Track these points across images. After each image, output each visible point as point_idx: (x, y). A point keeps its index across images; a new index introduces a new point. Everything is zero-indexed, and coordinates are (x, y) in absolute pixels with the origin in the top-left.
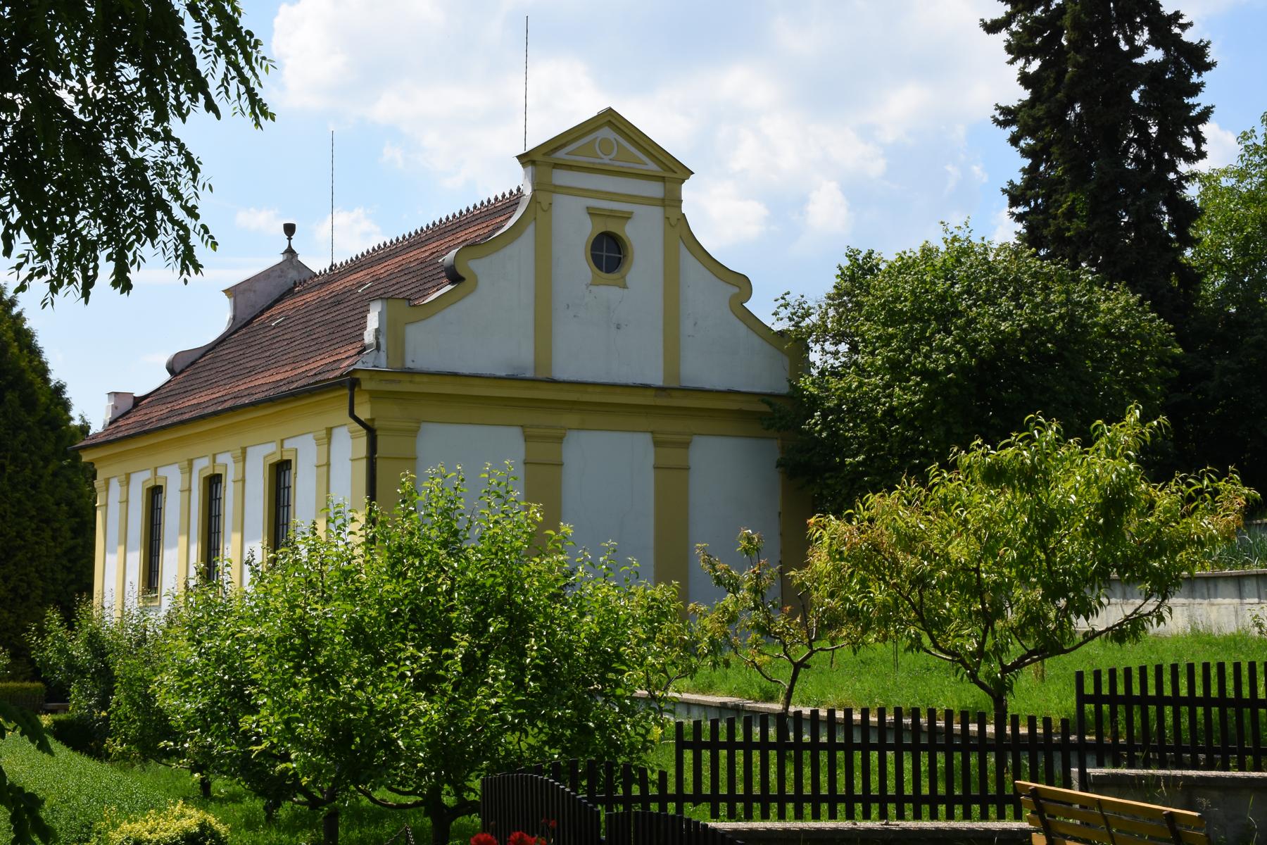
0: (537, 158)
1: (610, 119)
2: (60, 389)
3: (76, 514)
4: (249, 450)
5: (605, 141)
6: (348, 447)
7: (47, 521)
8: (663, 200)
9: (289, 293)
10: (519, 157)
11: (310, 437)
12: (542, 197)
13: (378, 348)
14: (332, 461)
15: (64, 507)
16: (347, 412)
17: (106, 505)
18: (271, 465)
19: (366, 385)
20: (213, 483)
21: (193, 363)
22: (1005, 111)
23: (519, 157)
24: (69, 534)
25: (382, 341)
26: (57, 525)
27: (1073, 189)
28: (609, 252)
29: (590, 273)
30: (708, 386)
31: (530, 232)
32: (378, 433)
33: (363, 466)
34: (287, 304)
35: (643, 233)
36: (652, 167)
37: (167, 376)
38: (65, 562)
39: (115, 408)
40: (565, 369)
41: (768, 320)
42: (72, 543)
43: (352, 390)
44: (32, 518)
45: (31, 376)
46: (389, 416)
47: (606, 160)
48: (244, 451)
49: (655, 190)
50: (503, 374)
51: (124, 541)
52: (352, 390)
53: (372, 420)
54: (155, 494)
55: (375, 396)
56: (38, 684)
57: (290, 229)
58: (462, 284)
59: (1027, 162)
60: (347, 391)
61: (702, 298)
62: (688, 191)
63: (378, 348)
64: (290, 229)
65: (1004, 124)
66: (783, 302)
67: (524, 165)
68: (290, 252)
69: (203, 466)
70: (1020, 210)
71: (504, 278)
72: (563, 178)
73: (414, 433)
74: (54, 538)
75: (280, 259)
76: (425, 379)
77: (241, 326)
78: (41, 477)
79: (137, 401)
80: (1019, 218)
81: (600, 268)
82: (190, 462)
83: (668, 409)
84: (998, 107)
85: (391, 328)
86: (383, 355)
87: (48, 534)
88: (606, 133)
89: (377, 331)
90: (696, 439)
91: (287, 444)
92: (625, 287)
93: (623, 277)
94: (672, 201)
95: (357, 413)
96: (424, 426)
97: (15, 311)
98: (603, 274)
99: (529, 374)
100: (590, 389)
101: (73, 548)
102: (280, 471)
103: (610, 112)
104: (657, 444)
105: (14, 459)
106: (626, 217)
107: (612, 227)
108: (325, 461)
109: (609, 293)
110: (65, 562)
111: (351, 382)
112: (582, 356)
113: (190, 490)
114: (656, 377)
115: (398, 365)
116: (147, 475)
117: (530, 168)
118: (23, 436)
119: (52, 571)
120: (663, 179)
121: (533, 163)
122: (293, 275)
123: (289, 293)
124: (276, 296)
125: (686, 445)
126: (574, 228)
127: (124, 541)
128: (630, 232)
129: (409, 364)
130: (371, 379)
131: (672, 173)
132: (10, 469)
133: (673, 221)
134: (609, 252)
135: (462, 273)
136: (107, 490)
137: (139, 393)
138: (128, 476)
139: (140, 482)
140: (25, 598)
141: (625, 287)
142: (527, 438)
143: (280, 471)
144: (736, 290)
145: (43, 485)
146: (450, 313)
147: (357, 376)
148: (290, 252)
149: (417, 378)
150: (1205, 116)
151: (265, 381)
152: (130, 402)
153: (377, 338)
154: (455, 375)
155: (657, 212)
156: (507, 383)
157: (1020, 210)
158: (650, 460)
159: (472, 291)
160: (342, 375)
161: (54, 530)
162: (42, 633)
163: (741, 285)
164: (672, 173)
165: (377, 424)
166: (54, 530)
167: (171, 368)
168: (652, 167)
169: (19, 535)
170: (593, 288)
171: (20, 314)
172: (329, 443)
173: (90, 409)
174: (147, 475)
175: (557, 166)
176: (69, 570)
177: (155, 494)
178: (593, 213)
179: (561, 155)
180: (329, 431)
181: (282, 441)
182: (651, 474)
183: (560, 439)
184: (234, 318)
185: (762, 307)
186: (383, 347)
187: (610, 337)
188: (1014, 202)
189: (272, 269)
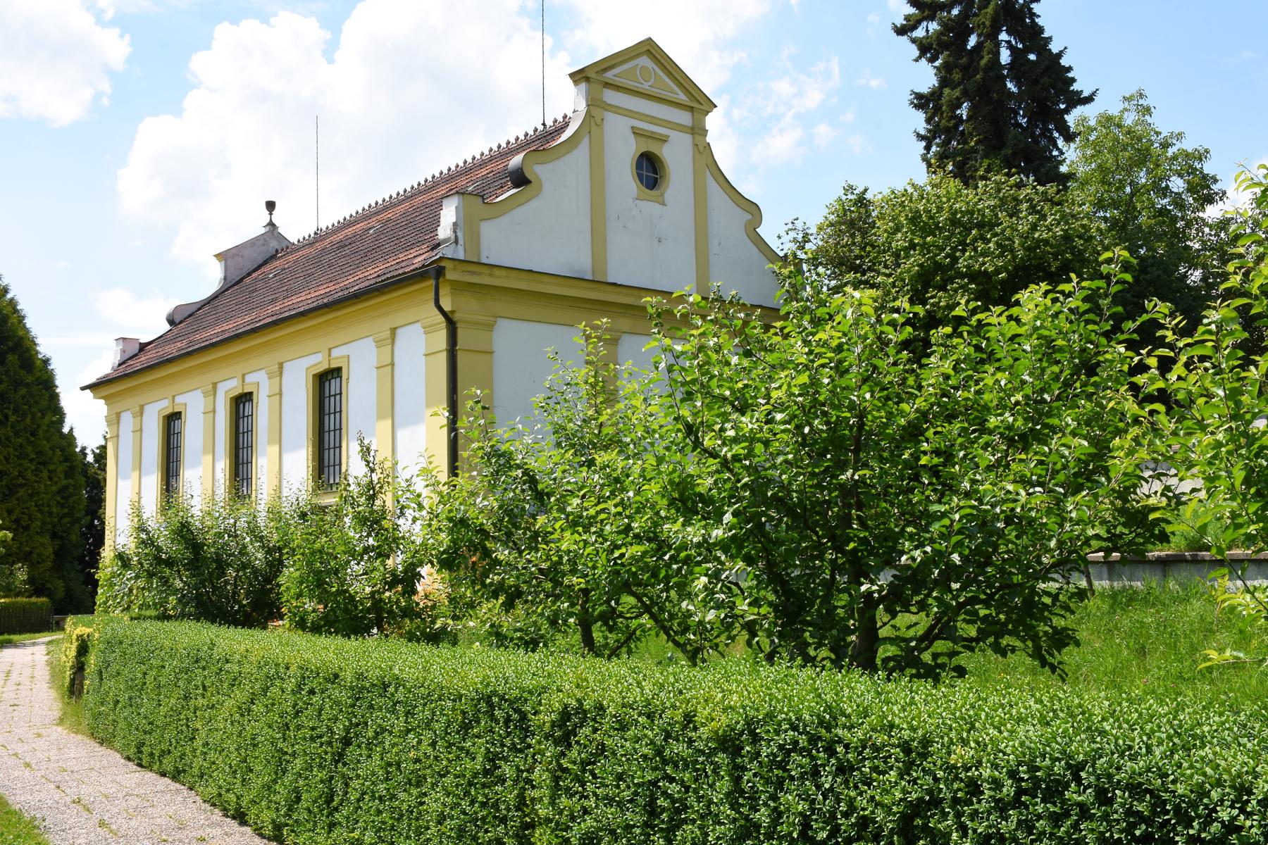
0: (591, 74)
1: (649, 49)
2: (46, 362)
3: (66, 460)
6: (417, 344)
7: (44, 464)
8: (692, 128)
9: (273, 257)
10: (572, 75)
13: (456, 242)
14: (396, 360)
15: (58, 452)
19: (450, 275)
20: (242, 401)
22: (919, 96)
23: (572, 75)
24: (62, 476)
25: (460, 235)
26: (52, 467)
27: (986, 156)
28: (650, 170)
31: (585, 144)
32: (458, 325)
33: (443, 359)
35: (676, 155)
36: (682, 97)
37: (168, 327)
38: (59, 499)
39: (124, 351)
40: (618, 273)
41: (774, 244)
42: (65, 482)
43: (437, 278)
44: (31, 461)
46: (466, 308)
49: (684, 118)
51: (139, 465)
52: (437, 278)
53: (453, 312)
54: (172, 420)
55: (458, 287)
56: (44, 599)
57: (271, 206)
58: (529, 187)
60: (433, 282)
61: (724, 218)
62: (713, 122)
63: (456, 242)
64: (271, 206)
66: (790, 226)
67: (576, 82)
68: (271, 224)
69: (230, 387)
71: (562, 182)
72: (611, 97)
73: (490, 327)
74: (50, 478)
75: (263, 231)
76: (503, 273)
77: (232, 285)
78: (39, 426)
79: (143, 347)
84: (913, 92)
85: (465, 224)
86: (461, 248)
87: (45, 474)
88: (645, 61)
89: (455, 224)
91: (335, 353)
93: (662, 195)
94: (698, 131)
95: (442, 303)
101: (65, 488)
105: (16, 411)
106: (663, 140)
107: (652, 147)
109: (650, 207)
110: (59, 499)
111: (435, 272)
117: (583, 86)
118: (23, 391)
119: (49, 506)
120: (691, 109)
121: (587, 79)
122: (274, 245)
123: (273, 257)
127: (139, 465)
130: (454, 269)
132: (13, 418)
133: (701, 149)
134: (650, 170)
135: (529, 175)
137: (144, 340)
140: (27, 528)
141: (664, 204)
144: (750, 217)
145: (41, 432)
146: (519, 213)
147: (443, 264)
148: (271, 224)
149: (496, 272)
152: (137, 348)
153: (455, 232)
155: (687, 139)
159: (537, 195)
160: (423, 266)
161: (50, 471)
163: (753, 211)
164: (699, 104)
165: (456, 317)
166: (50, 471)
167: (171, 321)
168: (682, 97)
169: (20, 474)
170: (638, 202)
171: (12, 299)
172: (393, 344)
175: (607, 85)
176: (62, 506)
177: (172, 420)
178: (637, 132)
179: (609, 75)
181: (330, 350)
184: (225, 278)
185: (774, 232)
186: (461, 241)
187: (650, 248)
189: (257, 238)
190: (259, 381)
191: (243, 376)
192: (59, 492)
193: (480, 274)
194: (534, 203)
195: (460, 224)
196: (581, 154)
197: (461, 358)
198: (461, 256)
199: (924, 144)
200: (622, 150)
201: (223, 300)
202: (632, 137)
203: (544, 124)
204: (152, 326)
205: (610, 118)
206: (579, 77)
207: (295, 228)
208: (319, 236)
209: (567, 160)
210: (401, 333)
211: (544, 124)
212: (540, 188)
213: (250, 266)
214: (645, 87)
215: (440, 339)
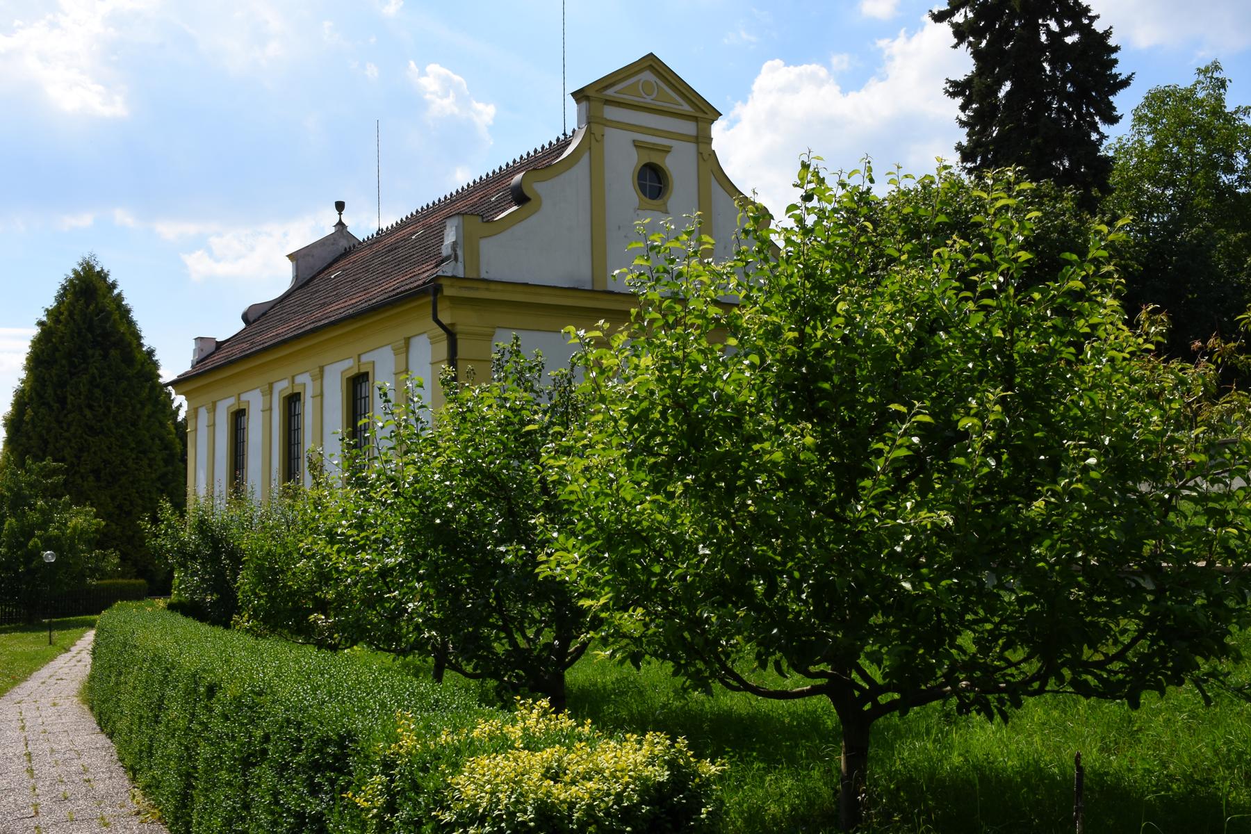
0: (591, 93)
1: (651, 63)
2: (151, 353)
3: (166, 448)
4: (327, 369)
5: (647, 83)
6: (426, 353)
7: (144, 452)
8: (697, 137)
11: (389, 348)
12: (595, 128)
15: (157, 442)
16: (430, 319)
17: (196, 430)
18: (348, 379)
20: (292, 401)
21: (264, 314)
22: (954, 84)
24: (161, 463)
25: (460, 253)
26: (152, 455)
28: (653, 182)
29: (637, 200)
31: (585, 158)
34: (342, 263)
35: (679, 165)
36: (686, 108)
37: (243, 325)
38: (159, 485)
44: (132, 450)
45: (129, 337)
46: (465, 320)
47: (648, 99)
48: (322, 369)
49: (689, 128)
53: (453, 325)
54: (238, 416)
56: (142, 581)
57: (340, 206)
58: (528, 205)
63: (456, 259)
64: (340, 206)
65: (953, 95)
68: (340, 224)
69: (282, 387)
70: (969, 165)
71: (563, 200)
72: (611, 113)
74: (150, 466)
75: (333, 230)
76: (500, 287)
78: (139, 417)
79: (219, 345)
81: (644, 193)
82: (271, 385)
84: (948, 81)
85: (468, 242)
86: (460, 265)
87: (145, 462)
88: (648, 76)
89: (455, 244)
91: (364, 358)
93: (665, 204)
95: (441, 317)
96: (498, 331)
97: (116, 292)
98: (647, 200)
99: (588, 287)
101: (165, 475)
102: (357, 384)
103: (651, 56)
106: (666, 150)
107: (655, 158)
108: (404, 368)
110: (159, 485)
111: (433, 289)
113: (271, 409)
115: (475, 276)
116: (231, 401)
117: (584, 104)
118: (124, 384)
120: (696, 119)
121: (587, 98)
122: (344, 244)
124: (329, 260)
128: (670, 164)
129: (484, 275)
130: (452, 286)
131: (704, 114)
132: (114, 410)
134: (653, 182)
135: (528, 194)
136: (196, 417)
138: (214, 404)
139: (224, 408)
140: (129, 513)
143: (357, 384)
146: (518, 229)
148: (340, 224)
149: (493, 287)
151: (338, 309)
152: (212, 347)
154: (526, 284)
155: (691, 148)
156: (570, 293)
157: (969, 165)
160: (424, 283)
162: (155, 520)
163: (763, 216)
165: (459, 328)
167: (245, 317)
168: (686, 108)
171: (119, 294)
172: (407, 352)
173: (173, 362)
174: (231, 401)
175: (608, 102)
177: (238, 416)
178: (637, 145)
179: (610, 92)
180: (407, 341)
184: (297, 277)
186: (460, 259)
188: (965, 158)
190: (305, 381)
191: (293, 377)
192: (159, 479)
193: (477, 289)
194: (534, 219)
195: (460, 242)
196: (581, 171)
199: (966, 130)
200: (623, 161)
201: (292, 299)
202: (634, 151)
203: (564, 134)
204: (228, 326)
205: (612, 135)
206: (579, 95)
207: (363, 226)
208: (381, 235)
209: (566, 176)
210: (414, 342)
211: (564, 134)
213: (320, 265)
214: (648, 100)
215: (443, 347)
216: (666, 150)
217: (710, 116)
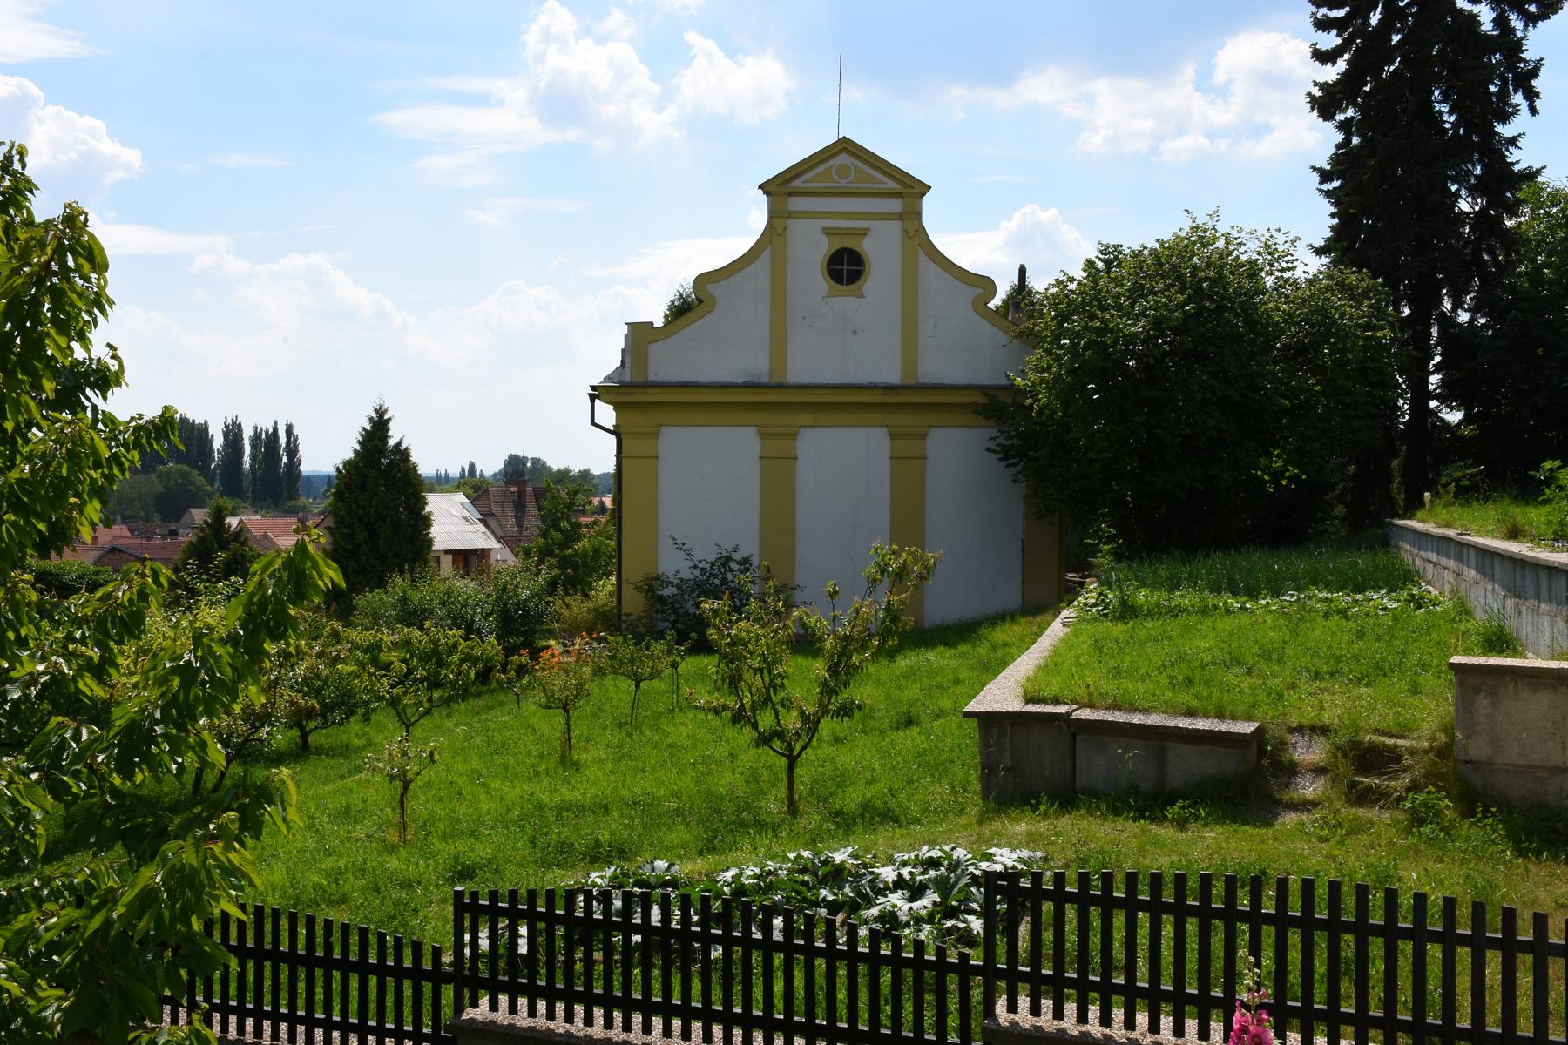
1: (845, 146)
5: (843, 167)
25: (627, 359)
28: (846, 267)
30: (948, 381)
35: (882, 248)
36: (891, 185)
40: (799, 372)
47: (843, 183)
49: (894, 205)
50: (740, 381)
59: (1340, 137)
62: (927, 202)
67: (767, 193)
72: (797, 204)
73: (656, 435)
80: (1328, 194)
83: (903, 405)
86: (627, 371)
88: (844, 159)
90: (934, 431)
92: (862, 296)
93: (860, 288)
94: (912, 216)
96: (664, 429)
99: (765, 380)
100: (816, 391)
104: (892, 436)
106: (864, 233)
107: (849, 243)
109: (844, 302)
112: (813, 362)
114: (892, 376)
115: (641, 379)
120: (900, 195)
125: (924, 436)
126: (811, 246)
128: (867, 247)
129: (652, 377)
134: (846, 267)
141: (862, 296)
142: (762, 435)
144: (981, 291)
149: (650, 390)
150: (1534, 73)
155: (896, 226)
158: (887, 452)
164: (912, 190)
168: (891, 185)
170: (830, 300)
175: (791, 194)
178: (828, 232)
179: (797, 184)
182: (887, 465)
183: (794, 436)
187: (849, 342)
197: (624, 462)
198: (628, 379)
205: (796, 225)
209: (745, 272)
212: (714, 305)
216: (864, 233)
217: (918, 190)
